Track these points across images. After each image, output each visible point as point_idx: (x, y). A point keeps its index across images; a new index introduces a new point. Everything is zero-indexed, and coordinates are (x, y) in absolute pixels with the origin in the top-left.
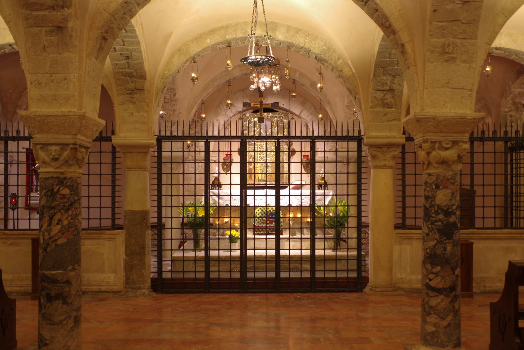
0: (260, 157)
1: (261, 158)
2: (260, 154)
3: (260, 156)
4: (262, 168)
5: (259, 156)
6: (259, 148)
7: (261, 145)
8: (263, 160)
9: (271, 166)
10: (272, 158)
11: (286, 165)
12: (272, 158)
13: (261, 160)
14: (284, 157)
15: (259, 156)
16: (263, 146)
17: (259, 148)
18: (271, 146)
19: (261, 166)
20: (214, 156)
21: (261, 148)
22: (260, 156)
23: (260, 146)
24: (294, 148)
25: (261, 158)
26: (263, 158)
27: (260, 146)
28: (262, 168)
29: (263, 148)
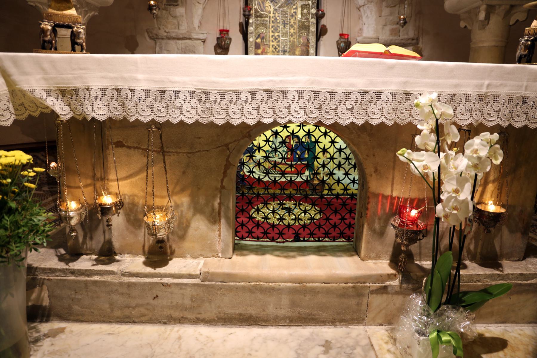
0: (272, 36)
1: (274, 37)
2: (272, 32)
3: (272, 34)
5: (271, 34)
7: (275, 16)
8: (277, 41)
9: (289, 51)
10: (292, 39)
11: (313, 50)
12: (292, 39)
13: (274, 40)
14: (310, 37)
15: (271, 34)
16: (278, 18)
17: (271, 22)
18: (290, 20)
19: (274, 50)
20: (201, 32)
21: (274, 21)
22: (272, 34)
23: (273, 19)
24: (325, 24)
25: (274, 37)
26: (277, 37)
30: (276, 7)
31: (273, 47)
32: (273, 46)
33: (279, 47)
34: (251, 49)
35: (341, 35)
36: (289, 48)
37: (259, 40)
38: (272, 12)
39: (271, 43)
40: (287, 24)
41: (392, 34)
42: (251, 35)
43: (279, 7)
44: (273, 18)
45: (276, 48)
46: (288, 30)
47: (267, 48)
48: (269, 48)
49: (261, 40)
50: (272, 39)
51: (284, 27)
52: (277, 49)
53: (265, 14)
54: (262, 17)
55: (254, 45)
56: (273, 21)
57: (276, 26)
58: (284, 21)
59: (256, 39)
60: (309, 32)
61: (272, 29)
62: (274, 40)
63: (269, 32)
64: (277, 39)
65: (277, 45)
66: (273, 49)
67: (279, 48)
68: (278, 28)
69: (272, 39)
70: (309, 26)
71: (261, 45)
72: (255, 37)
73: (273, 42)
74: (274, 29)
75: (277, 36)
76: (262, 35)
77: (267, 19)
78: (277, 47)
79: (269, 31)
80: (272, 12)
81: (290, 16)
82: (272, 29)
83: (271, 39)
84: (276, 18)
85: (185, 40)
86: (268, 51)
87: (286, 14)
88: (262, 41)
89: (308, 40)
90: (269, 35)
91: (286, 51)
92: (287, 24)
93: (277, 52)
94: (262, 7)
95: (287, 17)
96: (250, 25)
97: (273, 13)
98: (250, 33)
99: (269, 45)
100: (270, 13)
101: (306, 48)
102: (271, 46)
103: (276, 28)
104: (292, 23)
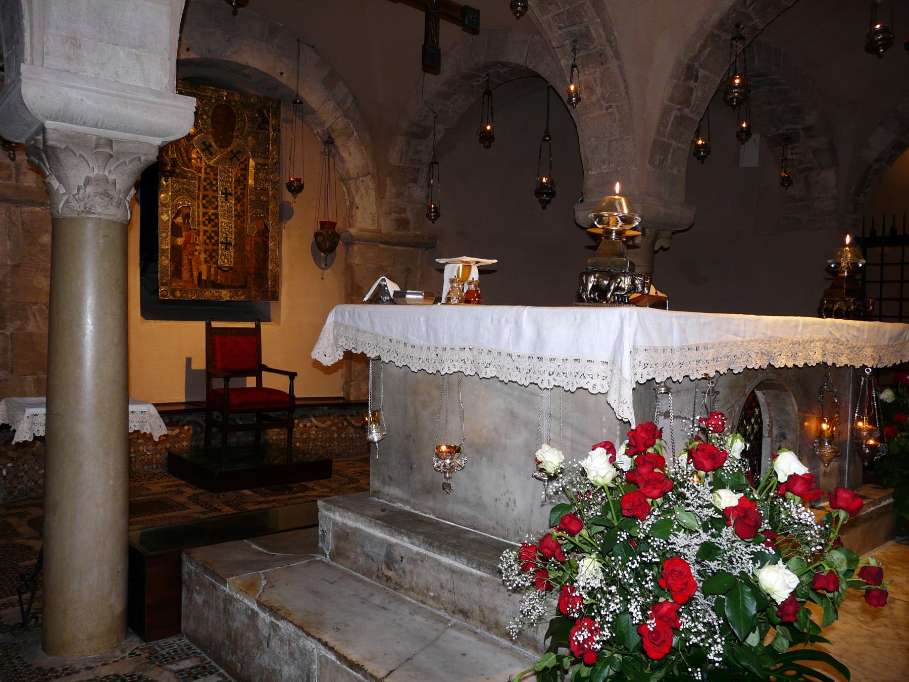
0: (204, 214)
3: (204, 210)
4: (210, 247)
6: (202, 188)
7: (209, 179)
9: (235, 244)
10: (238, 221)
17: (202, 188)
18: (236, 187)
19: (208, 241)
21: (208, 187)
22: (204, 210)
23: (205, 184)
26: (213, 217)
27: (205, 184)
28: (210, 247)
29: (215, 188)
30: (211, 163)
31: (205, 235)
32: (205, 232)
33: (217, 234)
34: (164, 235)
35: (323, 224)
36: (235, 239)
37: (179, 220)
38: (203, 171)
39: (203, 228)
40: (231, 194)
41: (399, 227)
42: (165, 209)
43: (217, 163)
44: (205, 181)
45: (210, 238)
46: (233, 205)
47: (194, 235)
48: (199, 235)
49: (184, 220)
50: (204, 219)
51: (226, 199)
52: (213, 238)
53: (190, 172)
54: (185, 178)
55: (170, 227)
56: (205, 187)
57: (210, 197)
58: (226, 189)
59: (175, 217)
60: (268, 214)
61: (204, 202)
62: (207, 222)
63: (198, 207)
64: (213, 220)
65: (213, 231)
66: (205, 237)
67: (216, 238)
68: (214, 200)
69: (204, 219)
70: (268, 202)
71: (183, 229)
72: (172, 213)
73: (205, 225)
74: (207, 202)
75: (213, 214)
76: (185, 211)
77: (195, 182)
78: (213, 235)
79: (198, 204)
80: (203, 171)
81: (235, 181)
82: (204, 202)
83: (201, 219)
84: (211, 182)
85: (29, 206)
86: (197, 242)
87: (229, 177)
88: (184, 222)
89: (266, 227)
90: (198, 213)
91: (230, 244)
92: (231, 194)
93: (213, 244)
94: (185, 158)
95: (230, 183)
96: (161, 189)
97: (206, 172)
98: (164, 205)
99: (199, 232)
100: (200, 172)
101: (263, 240)
102: (202, 233)
103: (210, 199)
104: (239, 194)
